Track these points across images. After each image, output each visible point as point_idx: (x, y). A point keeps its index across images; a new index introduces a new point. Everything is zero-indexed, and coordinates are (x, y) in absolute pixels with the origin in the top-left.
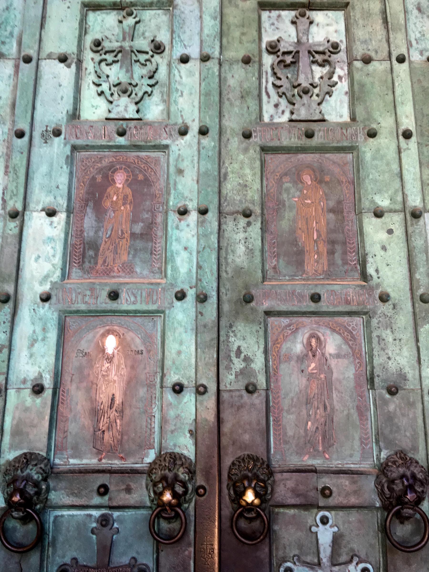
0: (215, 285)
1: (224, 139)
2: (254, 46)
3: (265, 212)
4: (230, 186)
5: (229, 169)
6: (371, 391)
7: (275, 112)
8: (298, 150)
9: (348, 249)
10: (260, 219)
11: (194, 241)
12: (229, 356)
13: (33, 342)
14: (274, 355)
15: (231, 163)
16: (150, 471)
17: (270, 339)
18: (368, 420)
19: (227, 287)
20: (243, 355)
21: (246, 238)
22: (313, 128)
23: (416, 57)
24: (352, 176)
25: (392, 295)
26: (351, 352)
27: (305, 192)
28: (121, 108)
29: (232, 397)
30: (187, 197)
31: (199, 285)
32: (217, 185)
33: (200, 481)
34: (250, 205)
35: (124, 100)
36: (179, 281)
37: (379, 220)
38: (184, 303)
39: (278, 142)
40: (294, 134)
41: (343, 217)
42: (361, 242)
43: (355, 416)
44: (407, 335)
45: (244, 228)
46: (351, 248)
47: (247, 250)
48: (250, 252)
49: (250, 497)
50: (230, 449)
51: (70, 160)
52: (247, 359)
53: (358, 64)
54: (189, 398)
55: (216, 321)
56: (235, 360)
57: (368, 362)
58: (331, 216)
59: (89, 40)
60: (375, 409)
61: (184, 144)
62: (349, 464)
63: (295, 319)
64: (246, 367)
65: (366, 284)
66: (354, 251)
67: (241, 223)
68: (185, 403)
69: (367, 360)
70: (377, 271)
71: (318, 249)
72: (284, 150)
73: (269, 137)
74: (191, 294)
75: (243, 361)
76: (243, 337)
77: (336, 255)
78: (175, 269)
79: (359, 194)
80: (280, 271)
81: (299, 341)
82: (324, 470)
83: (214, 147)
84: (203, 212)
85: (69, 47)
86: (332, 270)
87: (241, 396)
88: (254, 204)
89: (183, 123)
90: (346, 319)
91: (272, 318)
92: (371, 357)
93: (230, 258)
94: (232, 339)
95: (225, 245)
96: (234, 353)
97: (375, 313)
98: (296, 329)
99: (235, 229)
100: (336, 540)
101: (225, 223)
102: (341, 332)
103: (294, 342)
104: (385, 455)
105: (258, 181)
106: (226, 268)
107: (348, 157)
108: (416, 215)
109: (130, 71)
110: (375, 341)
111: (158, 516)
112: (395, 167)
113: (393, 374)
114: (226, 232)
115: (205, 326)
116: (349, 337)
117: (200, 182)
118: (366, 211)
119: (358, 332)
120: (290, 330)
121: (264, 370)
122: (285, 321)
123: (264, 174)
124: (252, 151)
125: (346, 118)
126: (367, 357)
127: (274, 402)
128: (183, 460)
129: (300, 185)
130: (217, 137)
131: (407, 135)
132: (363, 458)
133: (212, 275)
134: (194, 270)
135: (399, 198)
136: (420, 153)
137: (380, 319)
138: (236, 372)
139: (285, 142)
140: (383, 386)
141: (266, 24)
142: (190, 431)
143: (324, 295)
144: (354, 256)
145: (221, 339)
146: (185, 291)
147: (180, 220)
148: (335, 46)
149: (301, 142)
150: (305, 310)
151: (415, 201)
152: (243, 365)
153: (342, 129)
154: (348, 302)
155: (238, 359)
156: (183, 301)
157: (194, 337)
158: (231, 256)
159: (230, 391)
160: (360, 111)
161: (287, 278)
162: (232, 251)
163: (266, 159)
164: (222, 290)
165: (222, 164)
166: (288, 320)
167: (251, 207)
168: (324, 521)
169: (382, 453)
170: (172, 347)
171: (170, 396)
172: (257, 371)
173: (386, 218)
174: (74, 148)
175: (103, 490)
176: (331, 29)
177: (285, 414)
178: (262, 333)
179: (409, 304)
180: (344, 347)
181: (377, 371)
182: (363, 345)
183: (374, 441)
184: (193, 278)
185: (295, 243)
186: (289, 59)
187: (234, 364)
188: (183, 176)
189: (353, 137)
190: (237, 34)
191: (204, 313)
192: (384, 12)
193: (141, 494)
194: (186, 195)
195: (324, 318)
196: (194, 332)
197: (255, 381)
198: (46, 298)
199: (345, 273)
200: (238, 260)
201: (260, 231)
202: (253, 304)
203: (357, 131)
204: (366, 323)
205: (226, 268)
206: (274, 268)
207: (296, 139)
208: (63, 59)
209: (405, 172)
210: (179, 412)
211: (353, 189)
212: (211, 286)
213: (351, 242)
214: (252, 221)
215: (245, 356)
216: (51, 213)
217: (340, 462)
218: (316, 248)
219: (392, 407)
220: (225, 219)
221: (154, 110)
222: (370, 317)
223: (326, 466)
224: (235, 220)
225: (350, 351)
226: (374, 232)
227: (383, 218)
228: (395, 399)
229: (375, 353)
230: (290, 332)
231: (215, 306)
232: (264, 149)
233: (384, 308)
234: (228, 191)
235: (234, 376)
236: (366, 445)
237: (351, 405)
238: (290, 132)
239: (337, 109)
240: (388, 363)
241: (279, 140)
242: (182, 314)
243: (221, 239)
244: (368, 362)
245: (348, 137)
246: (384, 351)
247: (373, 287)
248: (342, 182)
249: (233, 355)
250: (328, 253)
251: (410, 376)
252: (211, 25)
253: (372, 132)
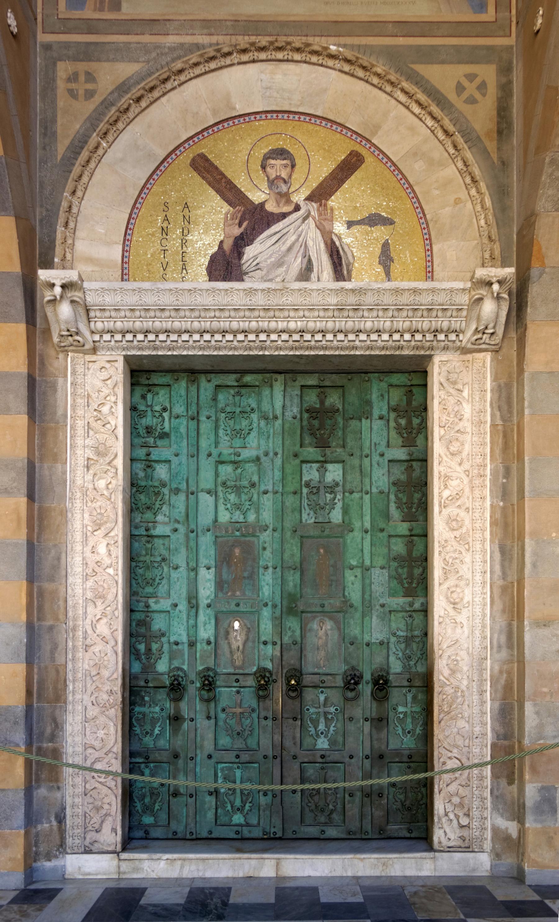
2: (298, 485)
3: (302, 568)
7: (308, 517)
11: (271, 581)
13: (205, 624)
16: (255, 674)
23: (374, 490)
28: (236, 517)
33: (274, 677)
35: (238, 512)
44: (359, 621)
48: (295, 586)
49: (293, 682)
51: (215, 543)
53: (347, 494)
54: (270, 647)
58: (331, 569)
59: (219, 480)
74: (270, 604)
78: (263, 593)
85: (210, 485)
100: (326, 699)
109: (240, 497)
111: (259, 689)
112: (360, 546)
125: (340, 521)
131: (366, 532)
141: (304, 471)
148: (337, 484)
160: (347, 518)
168: (322, 692)
170: (262, 626)
171: (262, 646)
173: (354, 570)
174: (216, 537)
175: (237, 681)
176: (336, 473)
186: (315, 490)
190: (290, 479)
192: (361, 466)
193: (251, 681)
198: (209, 606)
208: (209, 492)
216: (208, 568)
221: (252, 517)
226: (349, 576)
233: (352, 610)
239: (336, 516)
242: (266, 613)
252: (278, 474)
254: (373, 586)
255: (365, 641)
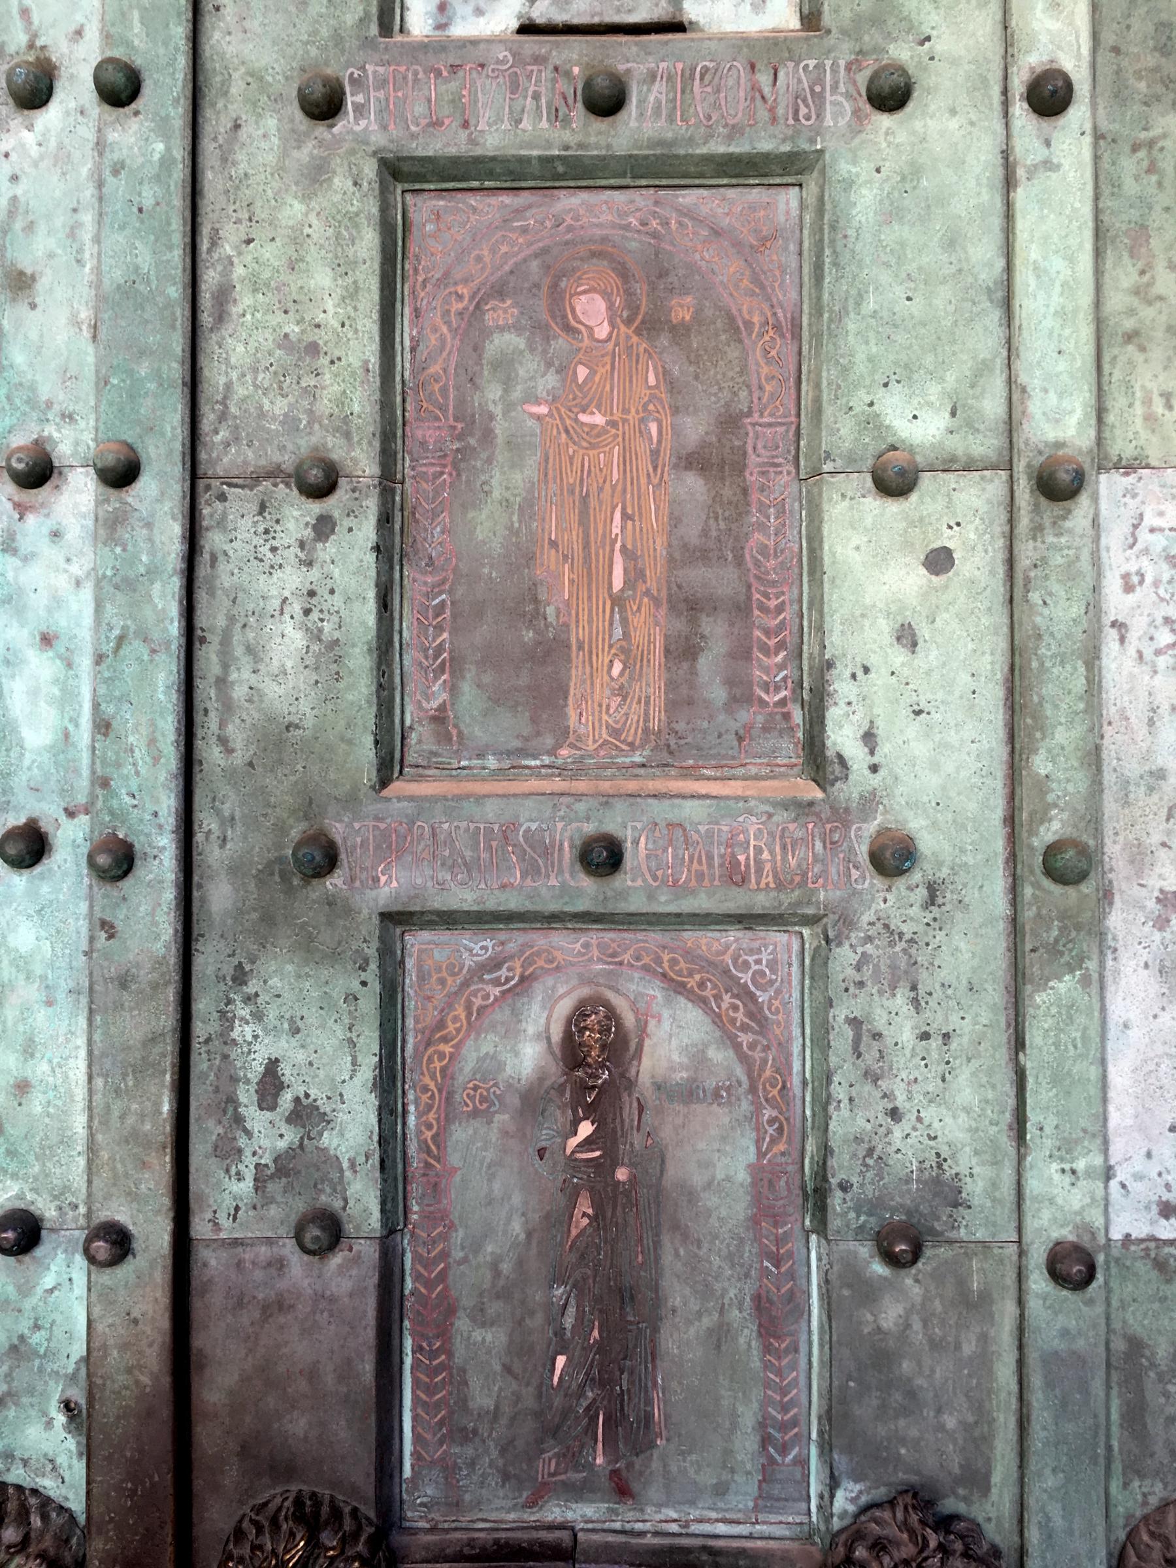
0: (168, 804)
1: (215, 123)
3: (394, 476)
4: (240, 349)
5: (239, 271)
6: (814, 1238)
8: (557, 177)
9: (757, 633)
10: (372, 505)
11: (82, 604)
12: (232, 1100)
14: (425, 1089)
15: (249, 241)
17: (410, 1023)
18: (796, 1350)
19: (226, 809)
20: (286, 1100)
21: (312, 594)
22: (622, 68)
24: (793, 295)
25: (926, 843)
26: (744, 1079)
27: (582, 372)
29: (239, 1265)
30: (49, 404)
31: (99, 804)
32: (178, 343)
34: (330, 441)
36: (20, 781)
37: (893, 507)
38: (42, 877)
39: (463, 135)
40: (536, 97)
41: (745, 491)
42: (810, 609)
43: (747, 1336)
44: (978, 1019)
45: (302, 545)
46: (767, 632)
47: (315, 647)
48: (327, 652)
50: (231, 1475)
52: (305, 1114)
55: (173, 960)
56: (256, 1118)
57: (809, 1124)
58: (693, 484)
60: (825, 1318)
61: (34, 151)
62: (709, 1521)
63: (516, 939)
64: (301, 1146)
65: (819, 795)
66: (781, 645)
67: (291, 525)
68: (51, 1291)
69: (808, 1112)
70: (869, 738)
71: (626, 635)
72: (491, 175)
73: (420, 109)
74: (70, 840)
75: (289, 1120)
76: (292, 1020)
77: (704, 663)
79: (818, 386)
80: (460, 734)
81: (531, 1030)
82: (607, 1546)
83: (166, 162)
84: (121, 474)
86: (681, 726)
87: (279, 1264)
88: (347, 435)
89: (31, 46)
90: (733, 936)
91: (426, 935)
92: (824, 1104)
93: (242, 677)
94: (243, 1031)
95: (221, 622)
96: (252, 1088)
97: (847, 922)
98: (523, 979)
99: (265, 550)
101: (221, 524)
102: (708, 993)
103: (512, 1033)
104: (853, 1500)
105: (369, 325)
106: (222, 725)
107: (782, 207)
108: (1058, 486)
110: (841, 1039)
112: (983, 253)
113: (908, 1181)
114: (223, 567)
115: (123, 982)
116: (740, 1016)
117: (103, 334)
118: (839, 463)
119: (778, 992)
120: (497, 982)
121: (375, 1159)
122: (476, 947)
123: (404, 290)
124: (341, 181)
126: (808, 1099)
127: (417, 1277)
128: (36, 1521)
129: (561, 343)
130: (178, 115)
131: (1049, 97)
132: (766, 1501)
133: (156, 760)
134: (84, 734)
135: (992, 406)
136: (1102, 183)
137: (869, 948)
138: (257, 1166)
139: (495, 136)
140: (861, 1228)
142: (68, 1406)
143: (636, 842)
144: (781, 667)
145: (200, 1030)
146: (45, 826)
147: (22, 510)
149: (567, 136)
150: (553, 907)
151: (1059, 419)
152: (290, 1136)
153: (753, 67)
154: (735, 876)
155: (268, 1115)
156: (38, 869)
157: (82, 1022)
158: (246, 674)
159: (236, 1243)
161: (492, 762)
162: (249, 650)
163: (413, 216)
164: (207, 822)
165: (204, 245)
166: (489, 943)
167: (337, 451)
169: (840, 1495)
172: (345, 1165)
177: (462, 1323)
178: (369, 1004)
179: (998, 885)
180: (719, 1056)
181: (842, 1167)
182: (796, 1049)
183: (814, 1436)
184: (77, 771)
185: (529, 608)
187: (249, 1134)
188: (33, 306)
189: (803, 111)
191: (119, 925)
194: (45, 391)
195: (640, 936)
196: (84, 1000)
197: (338, 1204)
199: (740, 739)
200: (274, 691)
201: (371, 558)
202: (335, 882)
203: (820, 81)
204: (813, 959)
205: (222, 725)
206: (439, 718)
207: (544, 124)
209: (1024, 278)
210: (24, 1326)
211: (793, 360)
212: (150, 807)
213: (773, 603)
214: (336, 514)
215: (297, 1100)
217: (674, 1515)
218: (618, 632)
219: (890, 1314)
220: (218, 505)
222: (828, 941)
223: (617, 1526)
224: (263, 508)
225: (740, 1072)
226: (869, 560)
227: (914, 497)
228: (909, 1282)
229: (839, 1092)
230: (497, 991)
231: (169, 895)
232: (399, 172)
233: (894, 903)
234: (234, 375)
235: (245, 1187)
236: (784, 1449)
237: (732, 1293)
238: (515, 87)
240: (889, 1132)
241: (466, 125)
243: (201, 596)
244: (809, 1124)
245: (780, 111)
246: (876, 1080)
247: (847, 810)
248: (749, 324)
249: (246, 1096)
250: (667, 651)
251: (975, 1189)
253: (887, 83)
254: (1116, 661)
255: (1047, 1227)
